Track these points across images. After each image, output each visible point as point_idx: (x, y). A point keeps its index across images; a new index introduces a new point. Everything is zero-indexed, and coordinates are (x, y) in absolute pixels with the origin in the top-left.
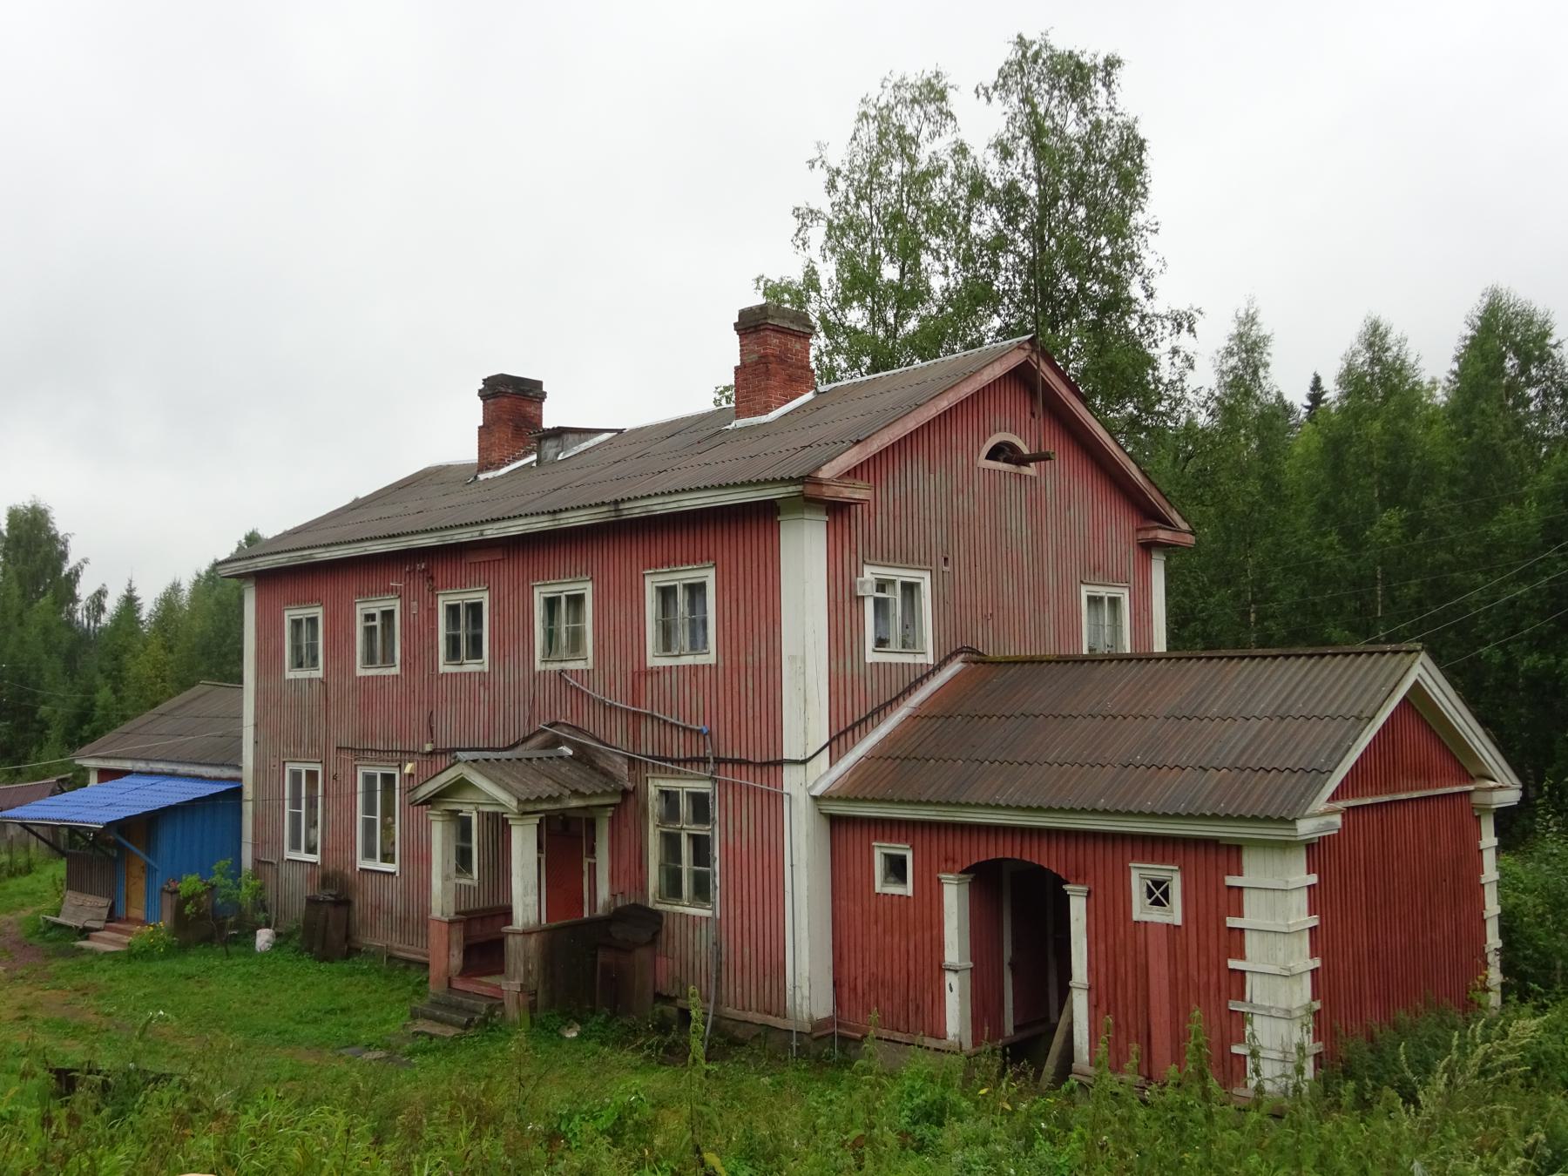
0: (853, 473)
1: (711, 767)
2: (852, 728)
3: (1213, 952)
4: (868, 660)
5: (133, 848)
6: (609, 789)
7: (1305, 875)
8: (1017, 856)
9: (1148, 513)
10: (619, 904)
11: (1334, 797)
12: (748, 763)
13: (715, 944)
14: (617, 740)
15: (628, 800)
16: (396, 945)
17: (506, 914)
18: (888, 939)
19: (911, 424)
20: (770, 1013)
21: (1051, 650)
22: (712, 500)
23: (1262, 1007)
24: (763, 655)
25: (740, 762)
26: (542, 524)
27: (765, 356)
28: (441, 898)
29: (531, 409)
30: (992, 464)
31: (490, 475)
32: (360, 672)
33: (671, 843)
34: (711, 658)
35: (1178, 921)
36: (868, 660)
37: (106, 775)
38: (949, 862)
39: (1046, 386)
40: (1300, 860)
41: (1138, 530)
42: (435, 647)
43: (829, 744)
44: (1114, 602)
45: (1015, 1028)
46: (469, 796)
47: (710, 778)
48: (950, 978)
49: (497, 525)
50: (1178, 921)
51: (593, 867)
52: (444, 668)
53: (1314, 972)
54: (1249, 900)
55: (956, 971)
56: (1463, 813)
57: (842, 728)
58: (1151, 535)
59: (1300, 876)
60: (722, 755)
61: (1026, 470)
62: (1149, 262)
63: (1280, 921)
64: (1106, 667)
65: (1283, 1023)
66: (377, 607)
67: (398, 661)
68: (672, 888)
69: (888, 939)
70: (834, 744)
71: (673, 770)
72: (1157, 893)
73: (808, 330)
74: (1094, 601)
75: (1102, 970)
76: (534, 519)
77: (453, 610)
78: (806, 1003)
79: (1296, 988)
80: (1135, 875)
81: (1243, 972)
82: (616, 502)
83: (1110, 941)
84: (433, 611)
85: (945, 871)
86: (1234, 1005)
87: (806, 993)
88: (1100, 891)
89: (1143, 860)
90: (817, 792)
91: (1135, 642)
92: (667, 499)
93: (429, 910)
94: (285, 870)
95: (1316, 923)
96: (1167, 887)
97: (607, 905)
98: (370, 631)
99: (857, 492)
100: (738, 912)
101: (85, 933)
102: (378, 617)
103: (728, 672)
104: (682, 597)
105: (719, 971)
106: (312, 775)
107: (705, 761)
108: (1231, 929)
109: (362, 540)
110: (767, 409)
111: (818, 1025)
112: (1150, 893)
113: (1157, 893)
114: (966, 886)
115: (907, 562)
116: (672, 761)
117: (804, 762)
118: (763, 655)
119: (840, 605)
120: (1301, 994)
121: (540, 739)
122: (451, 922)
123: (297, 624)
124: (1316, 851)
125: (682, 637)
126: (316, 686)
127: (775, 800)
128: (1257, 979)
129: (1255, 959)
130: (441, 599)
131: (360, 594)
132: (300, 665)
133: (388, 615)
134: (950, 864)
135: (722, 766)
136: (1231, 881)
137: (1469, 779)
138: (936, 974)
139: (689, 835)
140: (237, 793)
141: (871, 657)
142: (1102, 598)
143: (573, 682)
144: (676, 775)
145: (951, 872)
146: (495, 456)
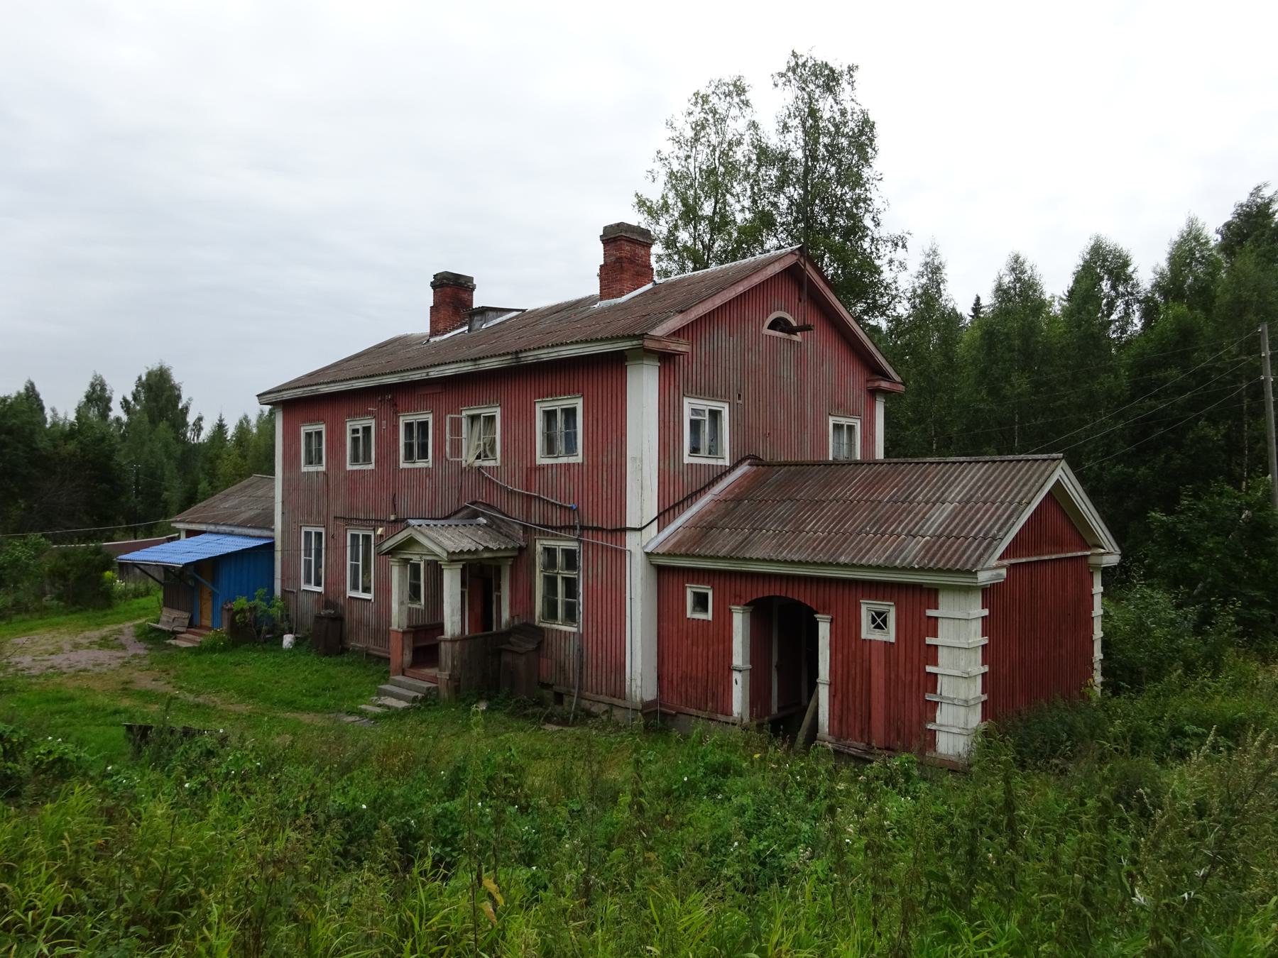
0: (677, 334)
1: (578, 532)
2: (673, 507)
3: (916, 661)
4: (686, 462)
5: (204, 581)
6: (509, 547)
7: (980, 610)
8: (783, 595)
9: (878, 372)
10: (516, 622)
11: (1001, 558)
12: (602, 529)
13: (579, 650)
14: (516, 514)
15: (522, 555)
16: (372, 647)
17: (440, 628)
18: (695, 648)
19: (718, 301)
20: (615, 697)
21: (808, 457)
22: (581, 350)
23: (948, 698)
24: (614, 457)
25: (597, 529)
26: (467, 367)
27: (621, 258)
28: (398, 616)
29: (465, 296)
30: (772, 332)
31: (438, 339)
32: (349, 467)
33: (551, 583)
34: (578, 458)
35: (893, 639)
36: (686, 462)
37: (191, 533)
38: (737, 599)
39: (810, 281)
40: (977, 599)
41: (868, 381)
42: (397, 451)
43: (659, 515)
44: (851, 428)
45: (779, 708)
46: (417, 550)
47: (577, 540)
48: (736, 676)
49: (438, 369)
50: (893, 639)
51: (499, 598)
52: (403, 465)
53: (984, 675)
54: (942, 626)
55: (740, 671)
56: (1083, 569)
57: (667, 507)
58: (877, 384)
59: (977, 610)
60: (585, 524)
61: (795, 338)
62: (877, 204)
63: (963, 640)
64: (846, 469)
65: (962, 711)
66: (360, 424)
67: (373, 461)
68: (551, 613)
69: (695, 648)
70: (661, 518)
71: (552, 534)
72: (879, 621)
73: (650, 242)
74: (838, 427)
75: (839, 672)
76: (462, 365)
77: (409, 426)
78: (639, 690)
79: (972, 686)
80: (864, 609)
81: (936, 675)
82: (517, 353)
83: (845, 652)
84: (396, 427)
85: (734, 604)
86: (929, 697)
87: (639, 684)
88: (840, 619)
89: (870, 598)
90: (648, 550)
92: (551, 350)
93: (390, 625)
94: (301, 597)
95: (987, 642)
96: (886, 617)
97: (508, 623)
98: (355, 440)
99: (681, 347)
100: (595, 629)
101: (174, 634)
102: (361, 431)
103: (590, 468)
104: (560, 417)
105: (581, 668)
106: (319, 535)
107: (574, 528)
108: (929, 645)
109: (350, 379)
110: (621, 294)
111: (646, 705)
112: (874, 621)
114: (748, 615)
115: (713, 396)
116: (552, 528)
117: (640, 529)
118: (614, 457)
119: (667, 424)
120: (975, 690)
121: (465, 512)
122: (404, 633)
123: (309, 435)
124: (989, 594)
125: (560, 445)
126: (321, 477)
127: (620, 555)
128: (945, 680)
129: (944, 666)
130: (401, 419)
131: (349, 416)
132: (311, 463)
133: (367, 430)
134: (738, 599)
135: (585, 532)
136: (930, 613)
137: (1088, 548)
138: (726, 673)
139: (563, 578)
140: (271, 546)
141: (688, 459)
142: (842, 425)
143: (487, 475)
144: (555, 537)
145: (738, 605)
146: (441, 326)
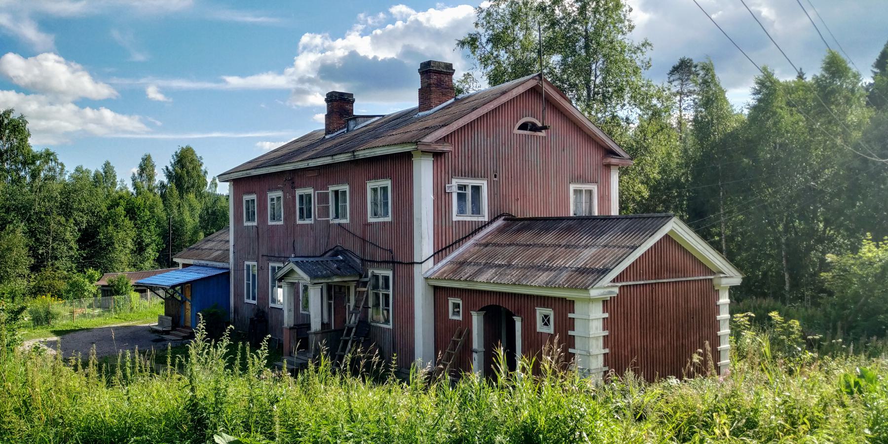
72: (546, 320)
90: (426, 276)
91: (600, 210)
112: (543, 320)
113: (546, 320)
125: (380, 210)
144: (378, 268)
